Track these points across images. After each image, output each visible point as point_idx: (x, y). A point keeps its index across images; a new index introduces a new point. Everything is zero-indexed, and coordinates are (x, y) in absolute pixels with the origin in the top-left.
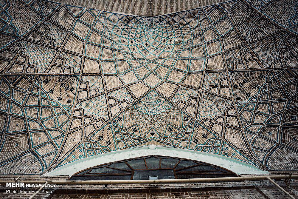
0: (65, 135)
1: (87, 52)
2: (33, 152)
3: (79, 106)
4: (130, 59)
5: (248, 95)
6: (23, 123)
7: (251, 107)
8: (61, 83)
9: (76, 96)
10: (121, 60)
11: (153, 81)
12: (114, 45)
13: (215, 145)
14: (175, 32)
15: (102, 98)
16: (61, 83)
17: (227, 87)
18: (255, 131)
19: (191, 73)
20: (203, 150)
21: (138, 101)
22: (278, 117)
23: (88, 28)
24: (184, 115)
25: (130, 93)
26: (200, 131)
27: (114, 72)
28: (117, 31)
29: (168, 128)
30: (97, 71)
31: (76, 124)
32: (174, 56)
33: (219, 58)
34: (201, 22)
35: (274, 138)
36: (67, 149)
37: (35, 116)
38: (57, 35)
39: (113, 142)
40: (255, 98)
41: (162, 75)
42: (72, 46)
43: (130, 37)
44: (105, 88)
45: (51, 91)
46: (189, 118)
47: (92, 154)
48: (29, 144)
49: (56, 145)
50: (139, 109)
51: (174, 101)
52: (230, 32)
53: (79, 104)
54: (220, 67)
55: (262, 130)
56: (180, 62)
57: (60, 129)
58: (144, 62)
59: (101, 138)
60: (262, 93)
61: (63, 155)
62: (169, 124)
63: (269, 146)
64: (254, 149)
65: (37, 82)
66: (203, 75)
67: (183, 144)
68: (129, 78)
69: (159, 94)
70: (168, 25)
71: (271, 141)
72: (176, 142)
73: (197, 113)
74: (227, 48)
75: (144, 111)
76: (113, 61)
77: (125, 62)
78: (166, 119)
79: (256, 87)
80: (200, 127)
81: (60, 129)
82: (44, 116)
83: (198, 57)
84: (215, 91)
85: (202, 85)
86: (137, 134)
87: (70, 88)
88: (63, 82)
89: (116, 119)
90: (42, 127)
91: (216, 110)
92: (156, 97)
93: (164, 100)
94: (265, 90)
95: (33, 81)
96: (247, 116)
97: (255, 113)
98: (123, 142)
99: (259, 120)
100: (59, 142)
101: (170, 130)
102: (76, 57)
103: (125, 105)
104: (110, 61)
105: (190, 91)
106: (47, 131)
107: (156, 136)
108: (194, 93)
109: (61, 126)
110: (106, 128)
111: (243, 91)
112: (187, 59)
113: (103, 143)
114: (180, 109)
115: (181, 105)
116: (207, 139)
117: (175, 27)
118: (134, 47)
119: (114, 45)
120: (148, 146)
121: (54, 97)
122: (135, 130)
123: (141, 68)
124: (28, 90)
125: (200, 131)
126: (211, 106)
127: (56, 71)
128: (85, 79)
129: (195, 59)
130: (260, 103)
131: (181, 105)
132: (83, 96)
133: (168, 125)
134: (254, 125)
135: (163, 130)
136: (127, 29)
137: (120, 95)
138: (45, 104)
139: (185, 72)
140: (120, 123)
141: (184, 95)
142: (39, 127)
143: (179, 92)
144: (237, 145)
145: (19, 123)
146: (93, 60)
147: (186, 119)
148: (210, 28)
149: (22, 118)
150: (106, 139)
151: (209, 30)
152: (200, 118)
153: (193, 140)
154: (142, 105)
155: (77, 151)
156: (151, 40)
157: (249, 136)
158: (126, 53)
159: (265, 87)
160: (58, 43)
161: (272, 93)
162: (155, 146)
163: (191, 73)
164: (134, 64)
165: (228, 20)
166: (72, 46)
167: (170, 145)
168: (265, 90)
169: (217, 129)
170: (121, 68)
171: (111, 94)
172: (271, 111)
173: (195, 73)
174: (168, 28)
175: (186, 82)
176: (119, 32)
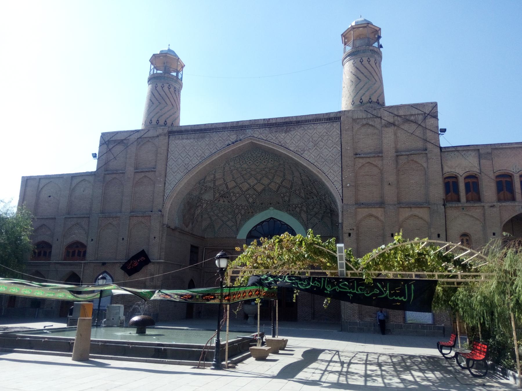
25: (255, 190)
36: (238, 223)
59: (249, 213)
63: (317, 221)
85: (291, 188)
103: (254, 196)
150: (251, 212)
169: (298, 210)
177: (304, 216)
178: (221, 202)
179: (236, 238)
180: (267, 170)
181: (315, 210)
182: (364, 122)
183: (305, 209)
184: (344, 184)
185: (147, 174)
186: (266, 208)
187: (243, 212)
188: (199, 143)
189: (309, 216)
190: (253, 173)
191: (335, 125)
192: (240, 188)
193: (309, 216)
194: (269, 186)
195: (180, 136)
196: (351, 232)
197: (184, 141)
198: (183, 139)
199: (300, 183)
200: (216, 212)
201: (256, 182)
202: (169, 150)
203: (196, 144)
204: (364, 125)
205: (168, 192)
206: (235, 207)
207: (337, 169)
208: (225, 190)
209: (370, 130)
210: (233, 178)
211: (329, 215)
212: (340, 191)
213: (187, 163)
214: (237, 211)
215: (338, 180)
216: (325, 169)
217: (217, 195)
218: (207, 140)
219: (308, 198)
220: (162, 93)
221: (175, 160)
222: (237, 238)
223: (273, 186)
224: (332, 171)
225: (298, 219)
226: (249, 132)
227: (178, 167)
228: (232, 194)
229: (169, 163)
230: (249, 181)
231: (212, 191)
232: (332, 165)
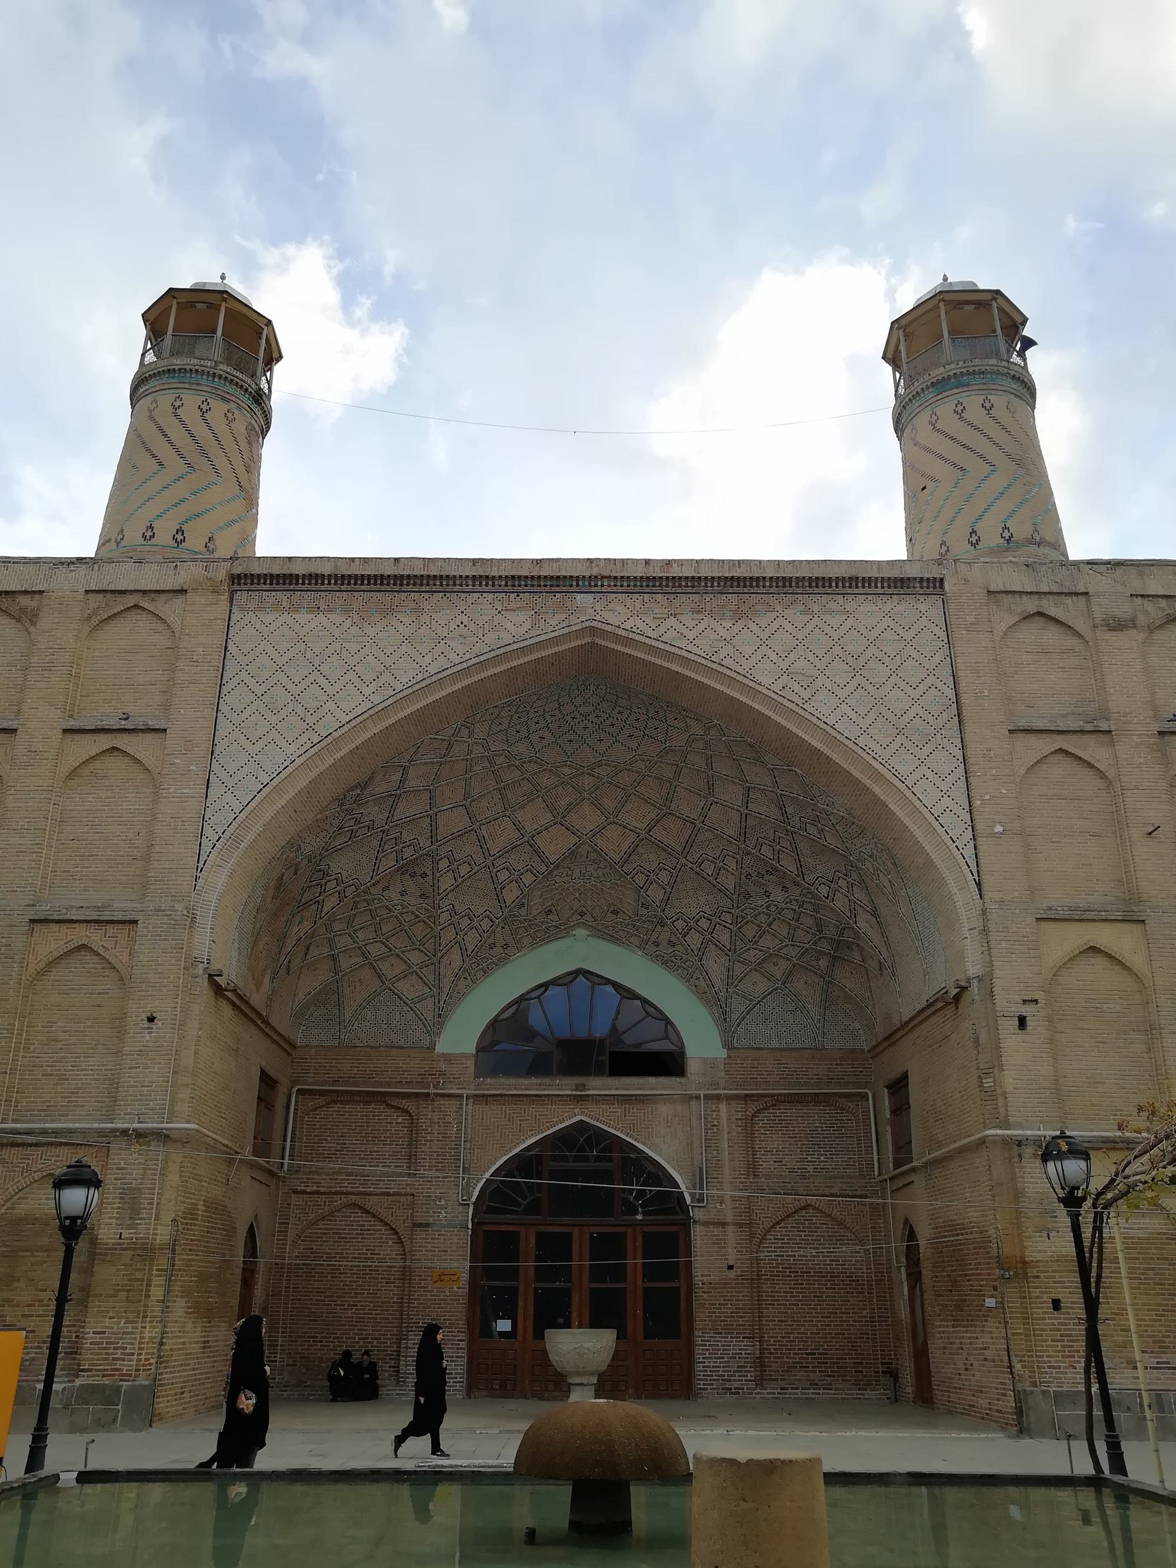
5: (767, 894)
11: (587, 818)
18: (753, 960)
25: (537, 852)
36: (446, 983)
48: (380, 977)
63: (763, 986)
75: (566, 879)
79: (785, 889)
85: (686, 851)
103: (528, 879)
113: (498, 950)
141: (651, 859)
164: (545, 780)
169: (694, 940)
175: (658, 832)
177: (715, 966)
178: (394, 895)
179: (432, 1047)
180: (602, 771)
181: (767, 942)
182: (1031, 605)
183: (725, 938)
184: (979, 826)
185: (121, 741)
186: (560, 931)
187: (471, 941)
188: (371, 632)
190: (545, 780)
191: (923, 607)
192: (481, 842)
193: (739, 969)
195: (283, 597)
196: (1027, 1010)
197: (303, 617)
198: (294, 609)
199: (732, 830)
200: (361, 935)
202: (231, 646)
203: (354, 630)
204: (1028, 617)
205: (219, 819)
206: (444, 917)
207: (946, 761)
208: (424, 842)
209: (1052, 637)
210: (466, 795)
211: (823, 963)
212: (969, 852)
213: (312, 705)
214: (448, 936)
215: (957, 810)
216: (904, 765)
217: (389, 862)
218: (407, 620)
219: (748, 896)
220: (201, 431)
221: (259, 690)
222: (440, 1048)
223: (614, 843)
224: (929, 774)
225: (688, 979)
226: (587, 607)
227: (274, 720)
228: (444, 864)
229: (231, 700)
230: (519, 815)
231: (375, 843)
232: (927, 749)
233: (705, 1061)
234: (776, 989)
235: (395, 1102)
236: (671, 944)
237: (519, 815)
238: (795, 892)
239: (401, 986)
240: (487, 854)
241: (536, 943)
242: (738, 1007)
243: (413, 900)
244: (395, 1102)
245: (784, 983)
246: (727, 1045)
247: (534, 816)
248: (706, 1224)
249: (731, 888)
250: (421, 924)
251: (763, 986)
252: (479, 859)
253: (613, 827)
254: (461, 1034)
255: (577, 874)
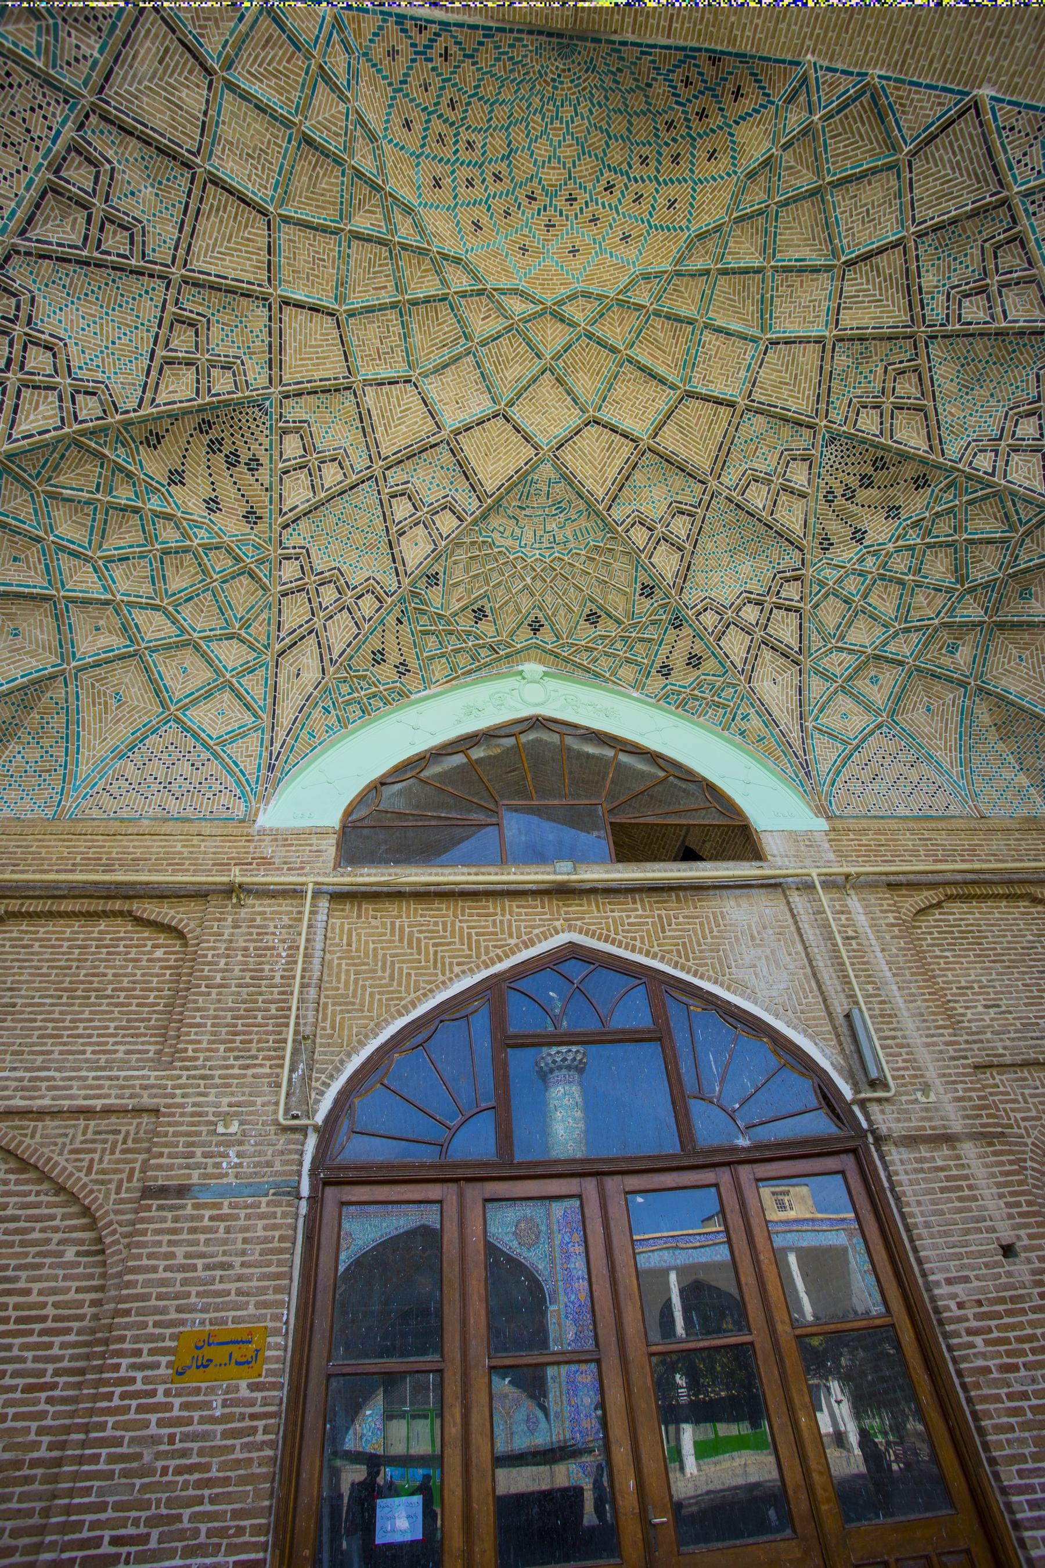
0: (269, 658)
1: (286, 273)
2: (178, 720)
3: (293, 539)
4: (463, 295)
5: (859, 536)
6: (117, 623)
7: (852, 586)
8: (206, 439)
9: (276, 496)
10: (427, 300)
11: (548, 417)
12: (398, 216)
13: (718, 700)
14: (665, 151)
15: (367, 495)
16: (206, 439)
17: (803, 495)
18: (838, 671)
19: (690, 395)
20: (682, 705)
21: (493, 506)
22: (914, 637)
23: (281, 132)
24: (643, 577)
26: (682, 645)
27: (399, 370)
28: (407, 124)
29: (587, 611)
30: (332, 368)
31: (295, 614)
32: (642, 296)
33: (809, 357)
34: (786, 147)
35: (878, 696)
36: (287, 713)
37: (146, 589)
38: (148, 192)
39: (413, 664)
40: (875, 553)
41: (585, 385)
42: (227, 251)
43: (465, 156)
44: (372, 448)
45: (176, 478)
46: (656, 590)
47: (359, 713)
48: (158, 693)
49: (249, 699)
50: (496, 535)
51: (617, 513)
52: (881, 251)
53: (290, 530)
54: (799, 403)
55: (858, 669)
56: (660, 330)
57: (242, 632)
58: (517, 307)
59: (379, 657)
60: (900, 543)
61: (281, 734)
62: (593, 600)
63: (858, 721)
64: (816, 734)
65: (121, 450)
66: (735, 421)
67: (627, 673)
68: (459, 400)
69: (568, 479)
70: (637, 103)
71: (868, 706)
72: (604, 665)
73: (685, 573)
74: (850, 320)
75: (510, 542)
76: (394, 305)
77: (444, 309)
78: (582, 581)
79: (893, 512)
80: (686, 631)
81: (242, 632)
82: (178, 582)
83: (735, 326)
84: (758, 498)
86: (485, 627)
87: (244, 459)
88: (214, 434)
89: (422, 584)
90: (183, 630)
91: (746, 567)
92: (558, 488)
93: (583, 506)
94: (914, 538)
95: (106, 452)
96: (831, 614)
97: (856, 611)
98: (444, 660)
99: (863, 636)
100: (255, 688)
101: (592, 618)
102: (244, 301)
104: (382, 308)
105: (678, 481)
106: (201, 642)
107: (546, 636)
108: (690, 493)
109: (246, 625)
110: (391, 620)
111: (843, 517)
112: (691, 322)
113: (386, 673)
114: (633, 554)
115: (639, 536)
116: (700, 672)
117: (670, 125)
118: (477, 213)
119: (398, 216)
120: (520, 668)
121: (189, 500)
122: (480, 614)
123: (504, 341)
124: (98, 490)
125: (682, 645)
126: (733, 552)
127: (178, 389)
128: (296, 411)
129: (719, 330)
130: (882, 577)
131: (639, 536)
132: (297, 493)
133: (589, 604)
134: (841, 649)
135: (569, 616)
136: (452, 105)
137: (429, 481)
138: (169, 535)
139: (673, 387)
140: (434, 596)
141: (653, 497)
142: (170, 629)
143: (637, 475)
144: (776, 713)
145: (101, 622)
146: (314, 309)
147: (648, 591)
148: (813, 193)
149: (107, 603)
150: (393, 658)
151: (807, 204)
152: (692, 596)
153: (657, 665)
154: (504, 521)
155: (317, 713)
156: (552, 176)
157: (817, 687)
158: (445, 257)
159: (916, 524)
160: (162, 235)
161: (928, 552)
162: (541, 668)
163: (690, 395)
165: (893, 182)
166: (227, 251)
167: (587, 670)
168: (914, 538)
169: (735, 645)
170: (430, 338)
171: (396, 476)
172: (904, 611)
173: (706, 399)
174: (635, 120)
175: (670, 440)
176: (417, 127)
177: (774, 686)
179: (249, 820)
187: (339, 633)
189: (817, 687)
194: (567, 455)
201: (480, 405)
208: (256, 374)
219: (826, 544)
223: (595, 463)
230: (432, 388)
233: (792, 836)
234: (879, 726)
235: (150, 910)
236: (694, 661)
237: (432, 388)
238: (916, 504)
239: (200, 716)
240: (373, 450)
241: (455, 677)
242: (825, 755)
243: (230, 525)
244: (150, 910)
245: (893, 713)
246: (821, 811)
247: (459, 400)
248: (911, 1141)
249: (798, 528)
250: (245, 580)
251: (858, 721)
252: (359, 460)
253: (594, 429)
254: (318, 794)
255: (529, 534)
